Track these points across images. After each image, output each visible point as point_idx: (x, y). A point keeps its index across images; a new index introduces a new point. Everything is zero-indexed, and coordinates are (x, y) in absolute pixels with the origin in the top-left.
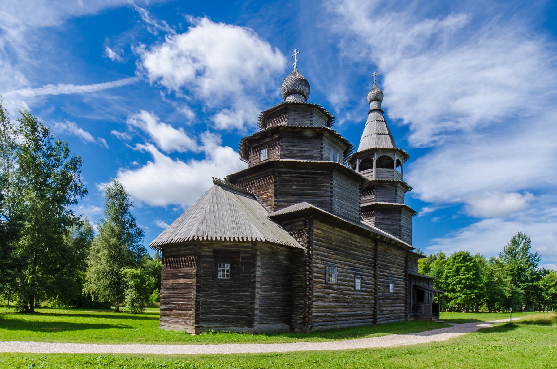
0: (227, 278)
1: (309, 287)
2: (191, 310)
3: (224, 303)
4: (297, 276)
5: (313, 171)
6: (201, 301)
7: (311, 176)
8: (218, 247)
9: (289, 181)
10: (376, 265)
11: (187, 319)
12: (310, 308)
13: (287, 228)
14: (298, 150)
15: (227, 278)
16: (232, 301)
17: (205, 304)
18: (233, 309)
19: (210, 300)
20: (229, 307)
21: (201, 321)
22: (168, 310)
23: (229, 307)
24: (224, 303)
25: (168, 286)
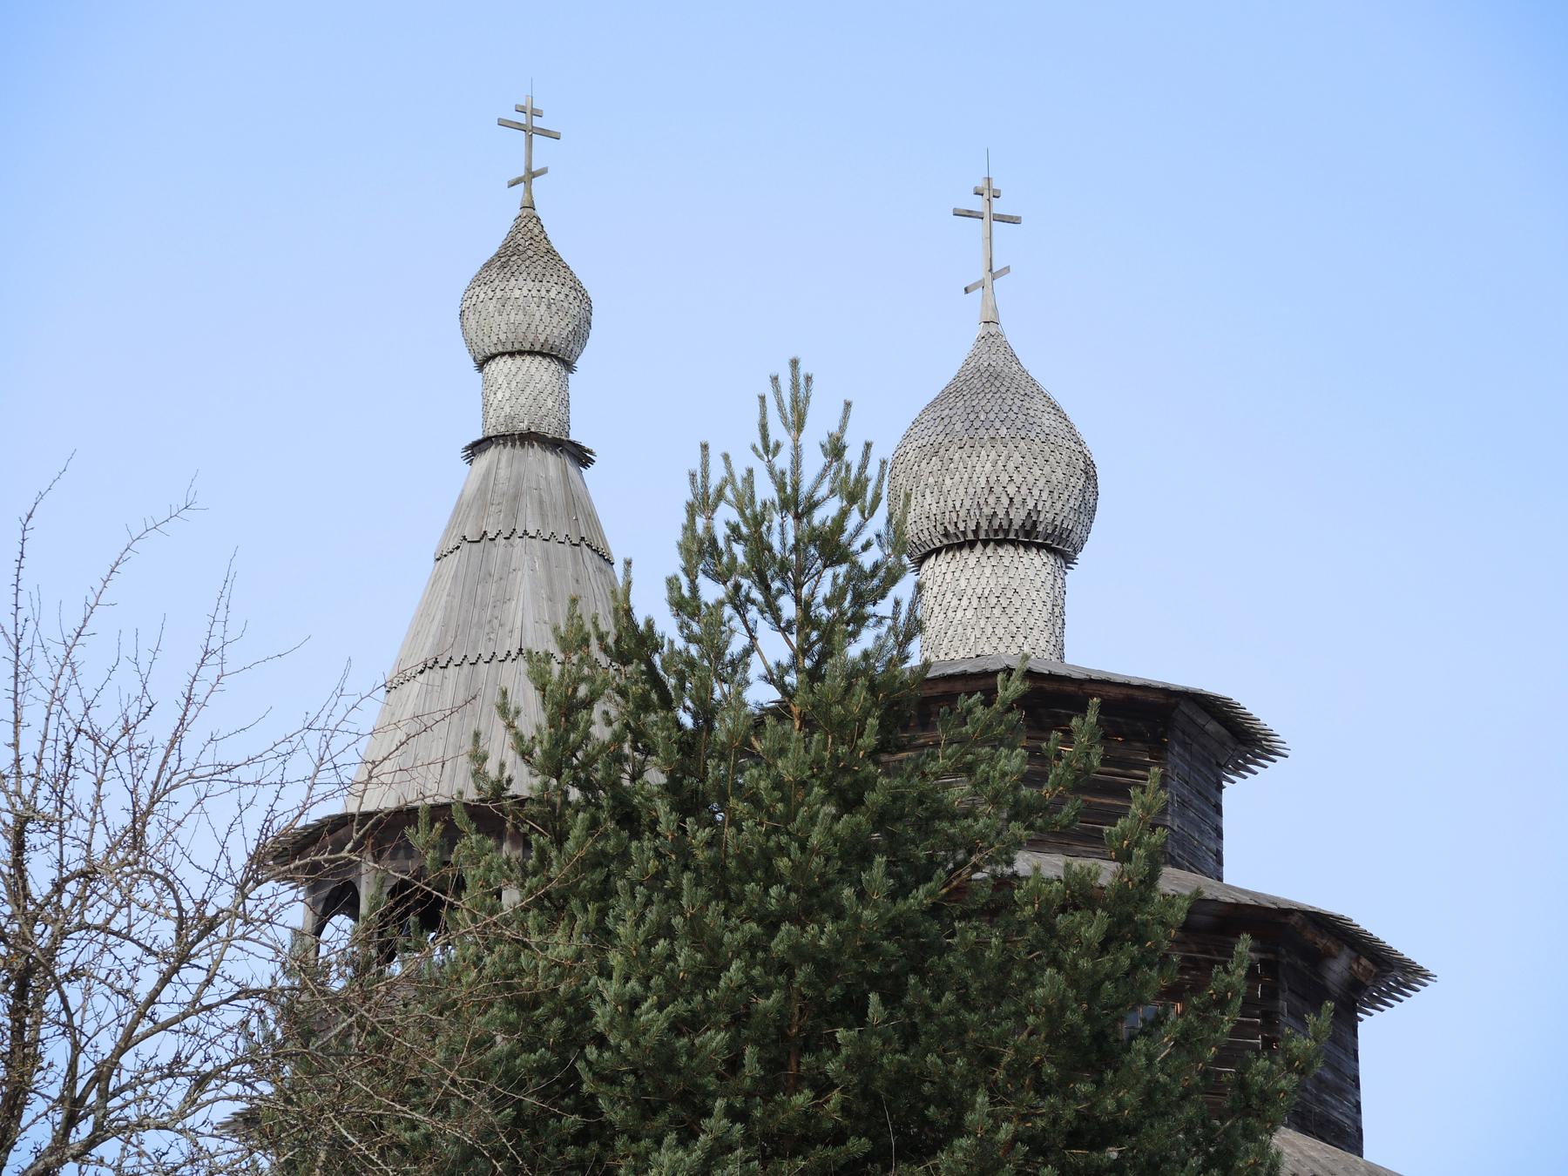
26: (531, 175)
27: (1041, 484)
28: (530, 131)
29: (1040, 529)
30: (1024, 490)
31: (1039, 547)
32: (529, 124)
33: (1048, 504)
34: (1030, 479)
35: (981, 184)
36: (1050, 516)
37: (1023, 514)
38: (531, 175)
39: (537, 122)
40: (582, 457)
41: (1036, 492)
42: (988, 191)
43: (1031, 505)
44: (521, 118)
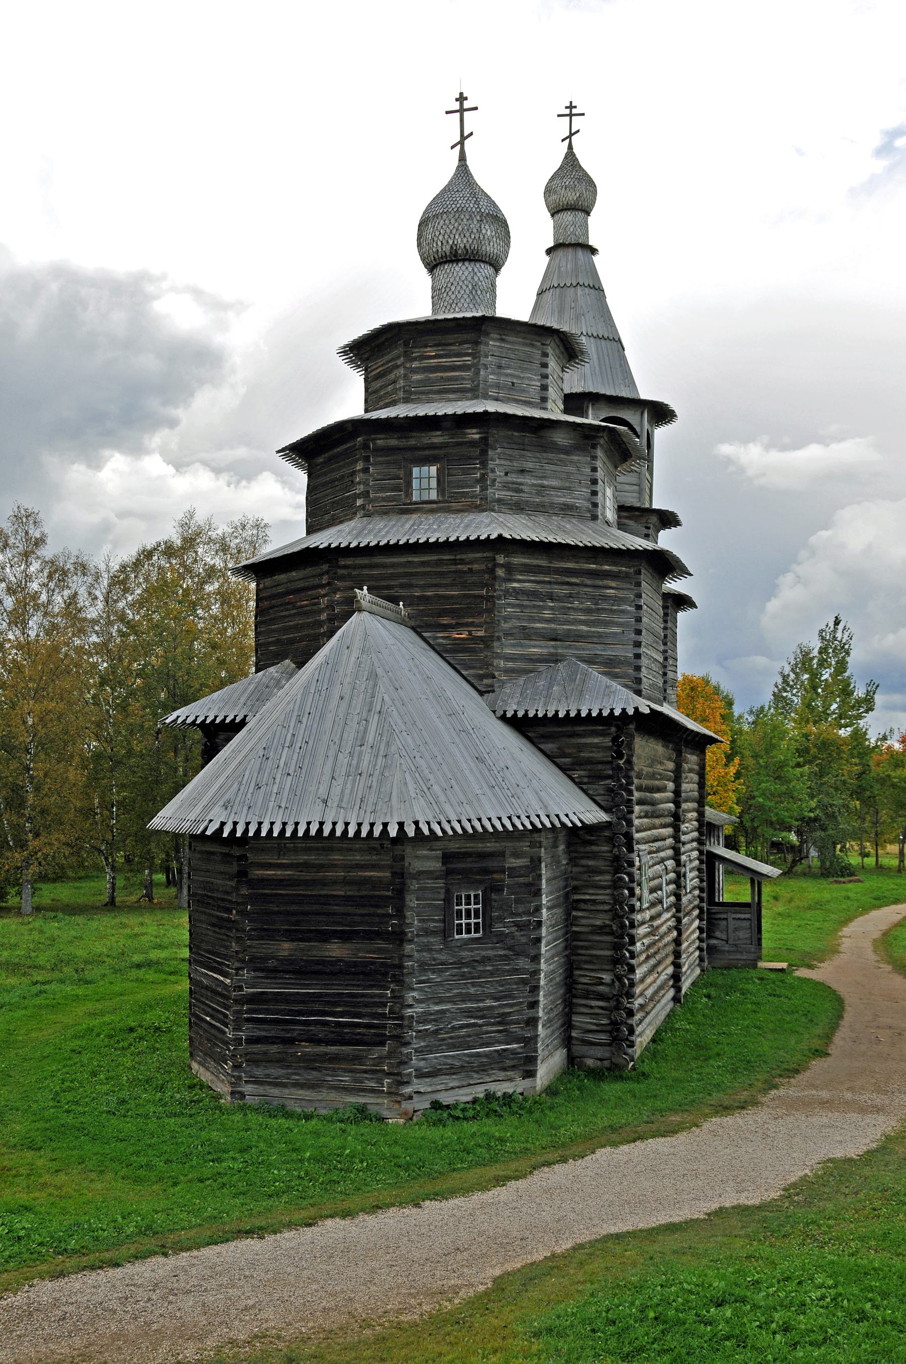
0: (477, 935)
1: (628, 935)
2: (382, 1044)
3: (469, 1013)
4: (588, 897)
5: (594, 566)
6: (417, 1013)
7: (589, 582)
8: (454, 846)
9: (533, 594)
10: (680, 821)
11: (365, 1072)
12: (630, 995)
13: (549, 747)
14: (533, 485)
15: (477, 935)
16: (489, 1003)
17: (425, 1022)
18: (490, 1028)
19: (437, 1008)
20: (480, 1022)
21: (417, 1077)
22: (273, 1043)
23: (480, 1022)
24: (469, 1013)
25: (271, 963)
26: (571, 135)
27: (454, 232)
28: (571, 115)
29: (460, 252)
30: (446, 237)
31: (464, 260)
32: (571, 112)
33: (459, 240)
34: (448, 231)
35: (458, 96)
36: (462, 245)
37: (448, 247)
38: (571, 135)
39: (574, 111)
40: (594, 251)
41: (452, 236)
42: (462, 98)
43: (451, 242)
44: (567, 111)
